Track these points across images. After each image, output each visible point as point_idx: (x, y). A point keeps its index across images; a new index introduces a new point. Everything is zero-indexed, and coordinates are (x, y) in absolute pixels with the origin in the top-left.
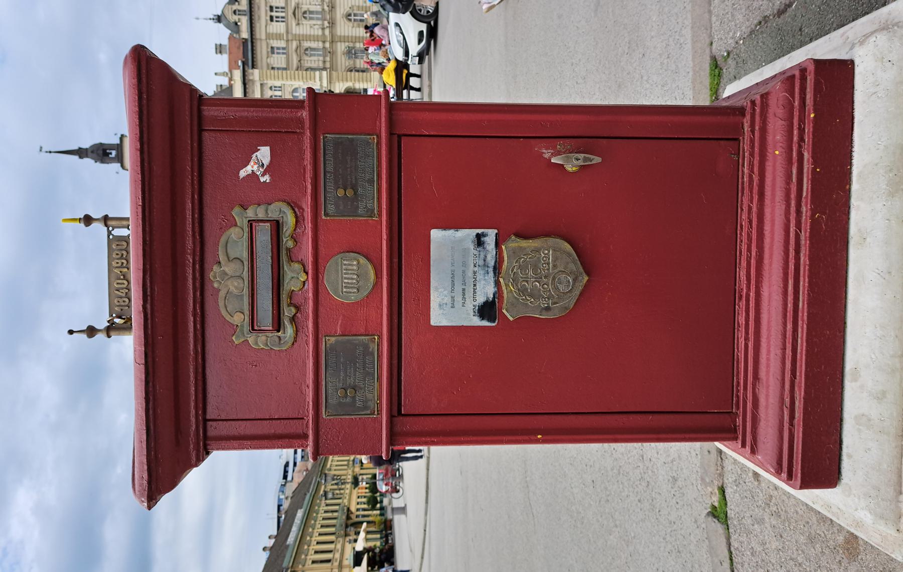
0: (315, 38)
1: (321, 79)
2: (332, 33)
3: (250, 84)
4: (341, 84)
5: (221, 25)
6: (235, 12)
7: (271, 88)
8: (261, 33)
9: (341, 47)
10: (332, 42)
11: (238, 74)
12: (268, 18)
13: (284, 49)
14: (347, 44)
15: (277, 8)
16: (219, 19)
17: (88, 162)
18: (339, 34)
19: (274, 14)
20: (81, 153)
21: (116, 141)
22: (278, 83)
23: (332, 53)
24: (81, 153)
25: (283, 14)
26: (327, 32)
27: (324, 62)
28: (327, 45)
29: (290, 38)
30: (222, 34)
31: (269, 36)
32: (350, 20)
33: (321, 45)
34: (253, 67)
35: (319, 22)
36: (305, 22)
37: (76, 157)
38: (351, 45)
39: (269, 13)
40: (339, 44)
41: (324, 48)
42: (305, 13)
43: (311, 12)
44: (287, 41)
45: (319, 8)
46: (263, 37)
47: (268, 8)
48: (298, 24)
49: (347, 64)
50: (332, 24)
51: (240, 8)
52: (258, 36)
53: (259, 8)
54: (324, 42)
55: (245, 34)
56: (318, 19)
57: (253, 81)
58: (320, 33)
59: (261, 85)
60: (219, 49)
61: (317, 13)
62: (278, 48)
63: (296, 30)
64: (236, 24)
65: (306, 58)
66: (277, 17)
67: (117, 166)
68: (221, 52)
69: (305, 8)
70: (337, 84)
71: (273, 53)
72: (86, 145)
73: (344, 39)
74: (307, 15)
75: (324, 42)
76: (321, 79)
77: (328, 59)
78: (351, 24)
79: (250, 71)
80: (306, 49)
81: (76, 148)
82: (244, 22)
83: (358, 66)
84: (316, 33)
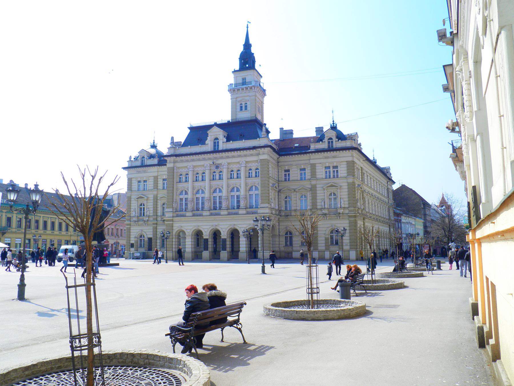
6: (331, 139)
8: (315, 159)
12: (327, 165)
13: (305, 178)
16: (334, 128)
17: (241, 49)
20: (247, 46)
24: (247, 46)
25: (332, 176)
27: (295, 210)
31: (313, 167)
36: (327, 193)
42: (335, 194)
43: (335, 199)
46: (312, 162)
51: (334, 142)
53: (334, 157)
55: (313, 147)
56: (330, 205)
57: (258, 154)
58: (319, 207)
60: (319, 130)
61: (336, 204)
62: (305, 173)
65: (298, 195)
66: (330, 172)
71: (301, 170)
74: (333, 197)
80: (305, 197)
81: (251, 42)
84: (318, 204)
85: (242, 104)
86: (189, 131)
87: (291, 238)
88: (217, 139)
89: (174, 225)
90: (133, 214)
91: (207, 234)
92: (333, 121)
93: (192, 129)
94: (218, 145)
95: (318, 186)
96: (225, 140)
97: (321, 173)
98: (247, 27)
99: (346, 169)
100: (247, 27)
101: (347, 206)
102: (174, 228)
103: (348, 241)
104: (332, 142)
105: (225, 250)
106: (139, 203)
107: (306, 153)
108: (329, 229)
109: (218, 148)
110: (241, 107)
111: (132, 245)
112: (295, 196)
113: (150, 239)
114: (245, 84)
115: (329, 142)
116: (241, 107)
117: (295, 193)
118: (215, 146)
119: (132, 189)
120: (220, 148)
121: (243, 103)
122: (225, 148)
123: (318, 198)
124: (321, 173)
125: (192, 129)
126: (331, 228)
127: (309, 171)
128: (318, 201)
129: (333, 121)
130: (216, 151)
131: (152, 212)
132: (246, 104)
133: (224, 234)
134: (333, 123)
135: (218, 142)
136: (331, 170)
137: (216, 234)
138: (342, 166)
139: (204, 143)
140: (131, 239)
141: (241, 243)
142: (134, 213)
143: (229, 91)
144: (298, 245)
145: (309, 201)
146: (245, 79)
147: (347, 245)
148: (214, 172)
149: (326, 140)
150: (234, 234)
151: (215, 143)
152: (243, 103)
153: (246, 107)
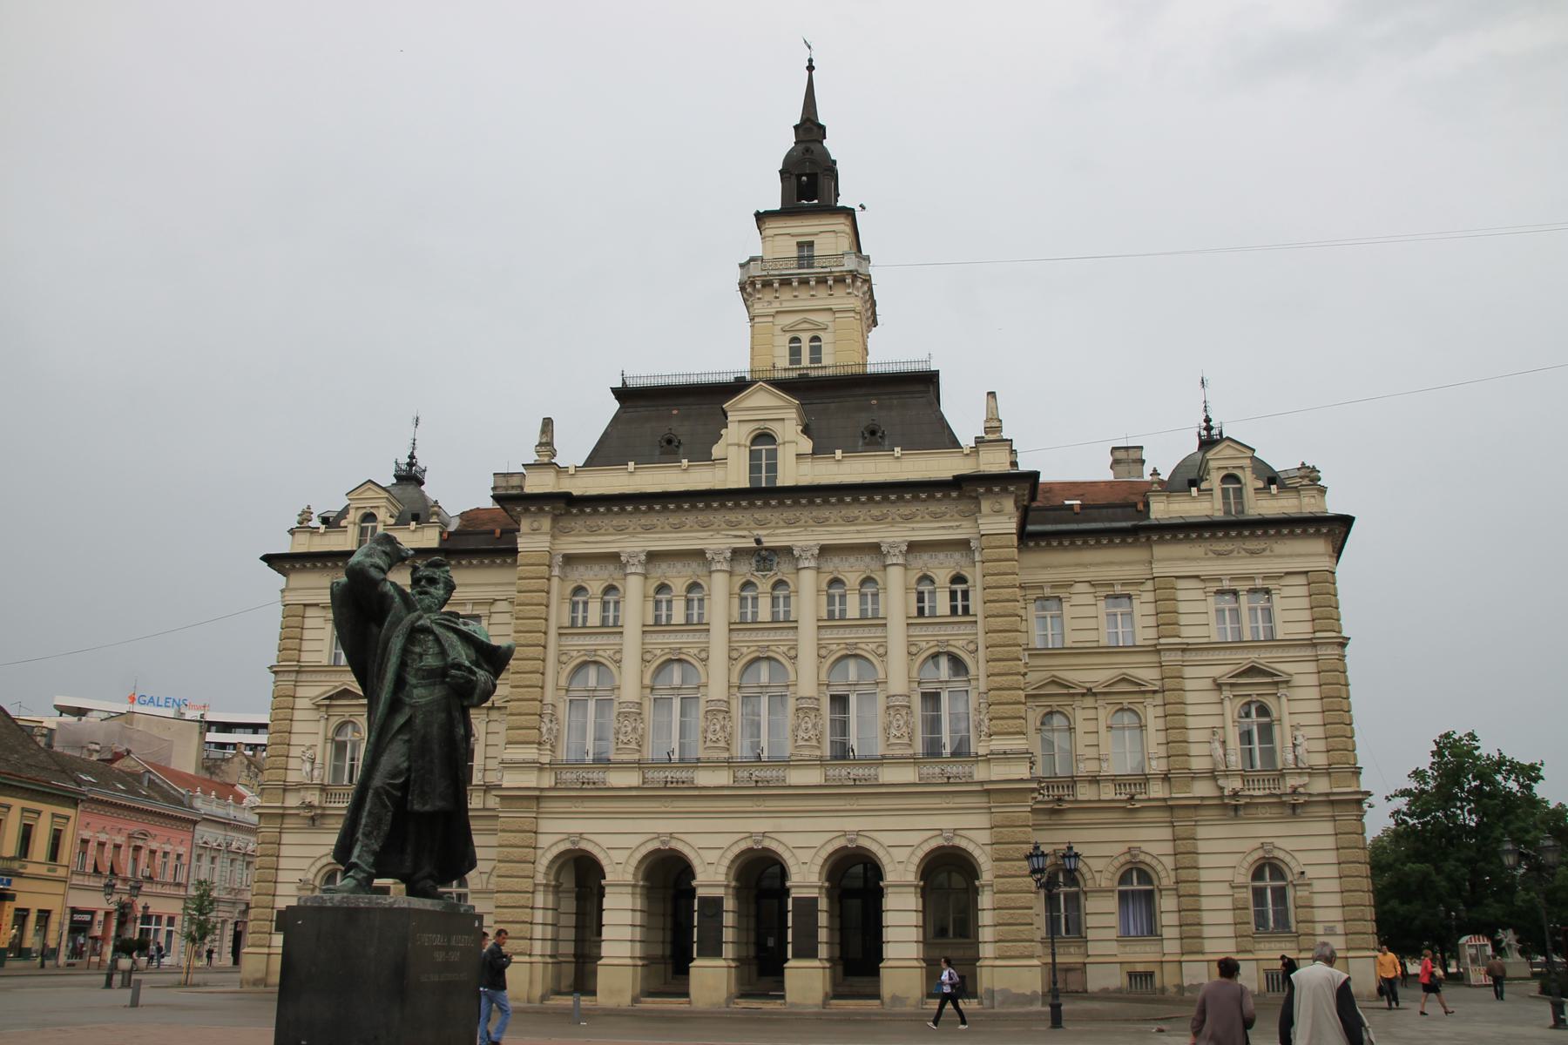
0: (1176, 744)
2: (1197, 806)
3: (963, 506)
4: (984, 837)
5: (1194, 446)
6: (1230, 478)
7: (958, 579)
8: (1171, 559)
9: (1153, 841)
10: (1169, 807)
14: (1169, 862)
15: (1268, 613)
17: (789, 141)
18: (1202, 832)
20: (810, 130)
23: (1129, 809)
24: (810, 130)
26: (1203, 789)
27: (1095, 780)
28: (1157, 790)
29: (1166, 657)
30: (1162, 460)
31: (1165, 589)
32: (1258, 874)
33: (1157, 766)
35: (1235, 760)
36: (1232, 708)
38: (1166, 879)
40: (1166, 833)
41: (1145, 779)
42: (1263, 711)
43: (1266, 732)
44: (1157, 650)
45: (1285, 757)
46: (1158, 569)
48: (1219, 686)
49: (1096, 865)
50: (1233, 808)
51: (1249, 492)
52: (1159, 551)
53: (1252, 553)
54: (1166, 778)
55: (1161, 510)
57: (974, 514)
58: (1198, 764)
59: (964, 545)
60: (1127, 457)
61: (1269, 754)
63: (1198, 678)
64: (1193, 483)
66: (1236, 612)
67: (777, 206)
68: (1116, 462)
70: (982, 820)
73: (1185, 853)
75: (1166, 778)
77: (1108, 792)
78: (1244, 877)
79: (1009, 504)
83: (1091, 905)
84: (1194, 749)
85: (795, 340)
86: (615, 405)
87: (1074, 901)
89: (545, 825)
90: (297, 773)
92: (1208, 420)
93: (624, 394)
94: (772, 468)
95: (1188, 672)
96: (806, 445)
97: (1201, 619)
98: (811, 68)
99: (1305, 603)
100: (811, 68)
101: (1320, 760)
102: (544, 841)
103: (1336, 915)
104: (1239, 493)
105: (813, 954)
106: (335, 721)
107: (1135, 531)
108: (1250, 859)
112: (1091, 714)
114: (811, 266)
115: (1225, 492)
117: (1089, 701)
118: (754, 468)
119: (305, 657)
120: (786, 478)
121: (805, 337)
122: (804, 481)
123: (1191, 722)
124: (1201, 619)
125: (624, 394)
126: (1256, 855)
127: (1150, 609)
128: (1193, 736)
129: (1208, 420)
130: (763, 494)
132: (816, 339)
133: (806, 876)
134: (1209, 429)
135: (773, 455)
137: (760, 874)
138: (1287, 592)
139: (703, 455)
140: (281, 889)
141: (888, 919)
142: (308, 767)
143: (742, 289)
144: (1113, 934)
145: (1154, 737)
146: (811, 244)
147: (1330, 932)
148: (748, 585)
149: (1214, 480)
150: (855, 878)
151: (754, 456)
152: (805, 337)
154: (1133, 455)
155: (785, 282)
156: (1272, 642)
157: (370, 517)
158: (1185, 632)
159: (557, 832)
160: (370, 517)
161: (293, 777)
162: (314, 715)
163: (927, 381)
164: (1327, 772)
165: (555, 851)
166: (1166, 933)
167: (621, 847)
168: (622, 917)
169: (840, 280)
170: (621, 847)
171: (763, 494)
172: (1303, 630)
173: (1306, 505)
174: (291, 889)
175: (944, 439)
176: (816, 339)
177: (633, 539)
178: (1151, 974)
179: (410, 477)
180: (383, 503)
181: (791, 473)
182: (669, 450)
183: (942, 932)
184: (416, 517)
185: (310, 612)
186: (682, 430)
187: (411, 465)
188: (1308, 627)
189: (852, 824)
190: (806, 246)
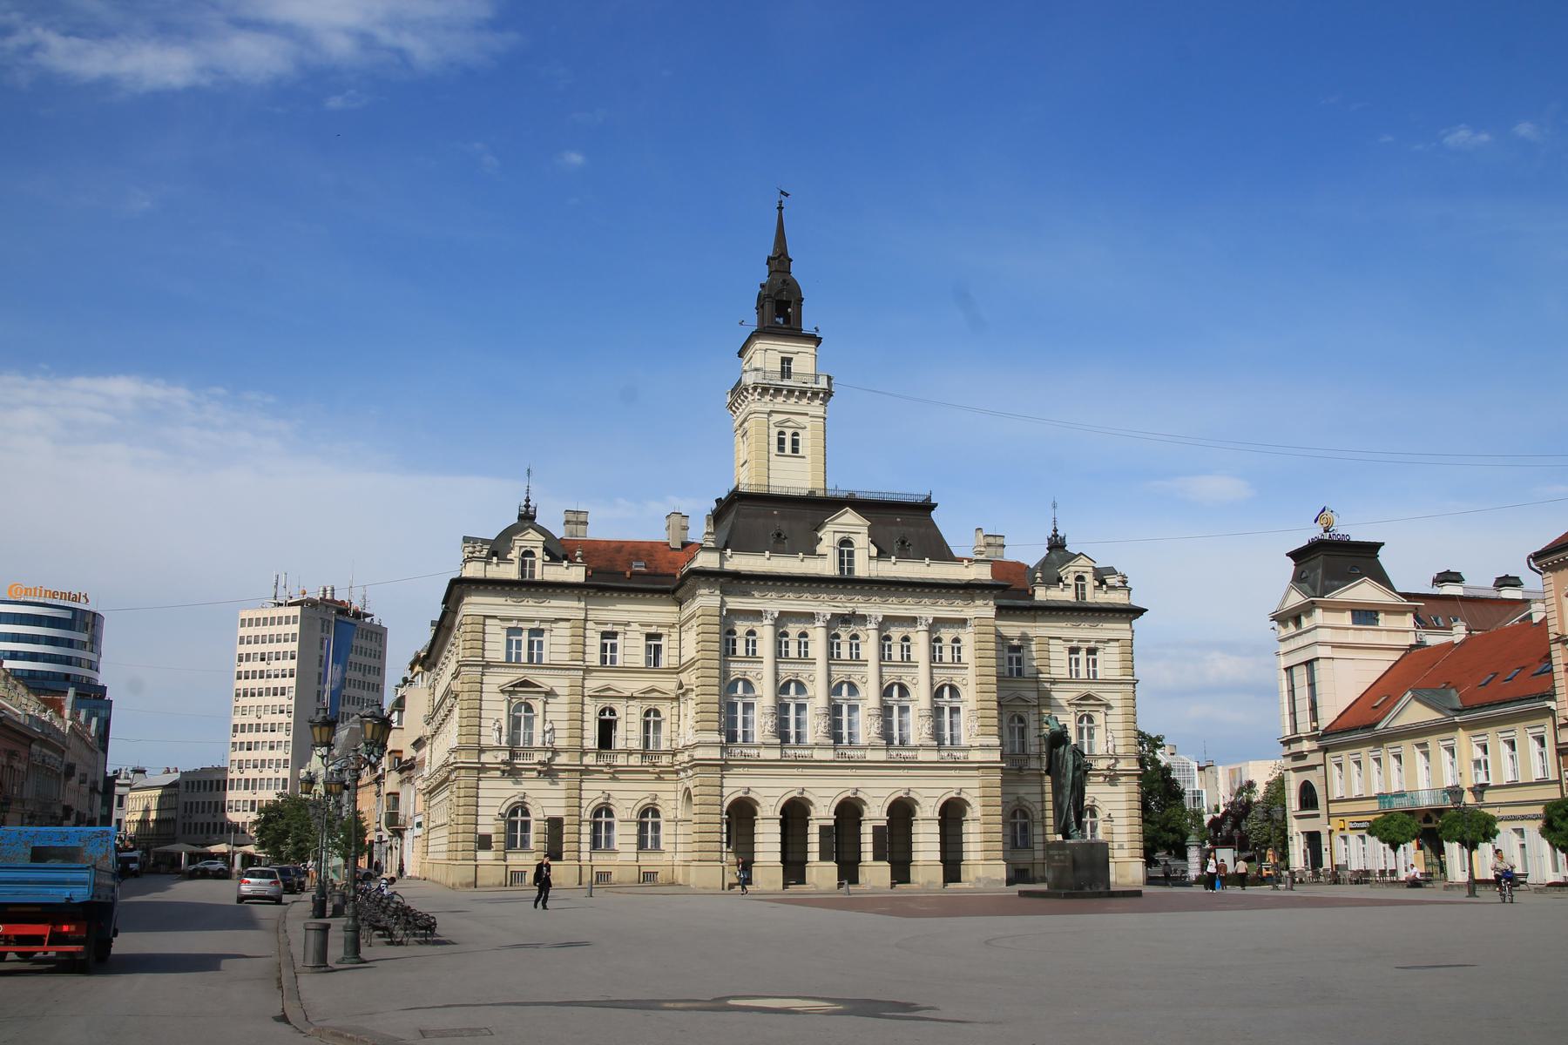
1: (984, 748)
11: (983, 573)
12: (1075, 644)
15: (1094, 661)
19: (1082, 655)
20: (780, 261)
21: (807, 327)
22: (968, 655)
24: (780, 261)
34: (1000, 608)
37: (769, 251)
39: (1084, 645)
47: (1092, 644)
55: (1041, 594)
66: (1077, 661)
69: (1099, 718)
70: (976, 783)
72: (796, 271)
76: (984, 748)
80: (1021, 720)
82: (1066, 595)
88: (846, 542)
91: (822, 813)
94: (851, 562)
98: (780, 208)
99: (1118, 657)
100: (780, 208)
102: (726, 792)
109: (851, 570)
110: (781, 442)
111: (484, 842)
113: (555, 825)
116: (781, 442)
118: (841, 562)
119: (487, 654)
121: (789, 432)
131: (565, 733)
135: (851, 554)
136: (1082, 655)
146: (789, 360)
147: (1121, 847)
151: (841, 553)
152: (789, 432)
153: (795, 443)
154: (999, 541)
155: (778, 391)
156: (1094, 680)
157: (529, 553)
158: (1053, 670)
159: (734, 787)
160: (529, 553)
161: (484, 741)
162: (501, 697)
163: (927, 507)
164: (1125, 757)
165: (732, 798)
166: (1036, 847)
167: (770, 795)
168: (768, 839)
169: (815, 394)
170: (770, 795)
171: (845, 582)
172: (1115, 674)
173: (1117, 598)
174: (490, 820)
175: (942, 553)
176: (795, 434)
177: (772, 604)
178: (1026, 871)
179: (527, 518)
180: (540, 544)
181: (865, 565)
182: (779, 544)
183: (1014, 845)
184: (565, 557)
185: (488, 621)
186: (784, 526)
187: (527, 506)
188: (1118, 672)
189: (905, 784)
190: (786, 361)
